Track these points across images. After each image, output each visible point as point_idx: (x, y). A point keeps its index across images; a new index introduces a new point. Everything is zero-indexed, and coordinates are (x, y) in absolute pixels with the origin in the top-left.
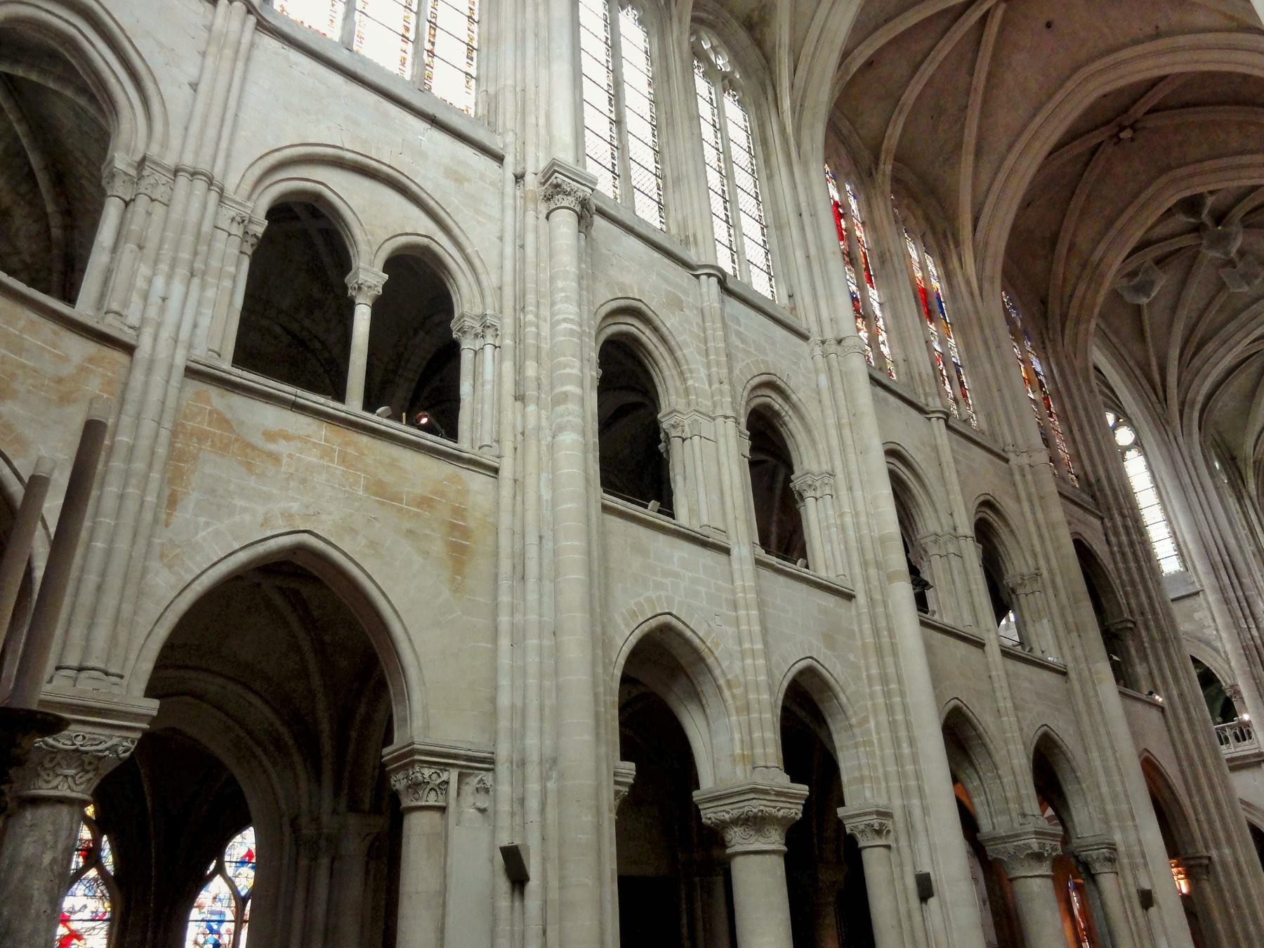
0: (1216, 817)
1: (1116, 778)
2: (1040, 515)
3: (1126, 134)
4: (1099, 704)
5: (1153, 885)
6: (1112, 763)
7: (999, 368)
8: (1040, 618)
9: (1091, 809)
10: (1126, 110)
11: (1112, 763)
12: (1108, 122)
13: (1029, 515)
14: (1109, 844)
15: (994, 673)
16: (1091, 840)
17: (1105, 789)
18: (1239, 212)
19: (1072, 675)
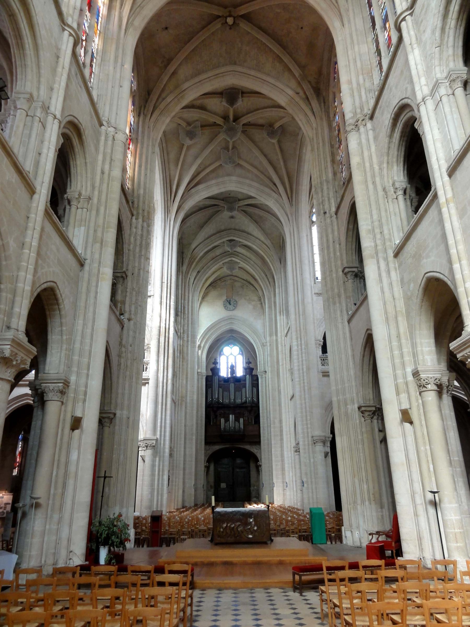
0: (127, 392)
1: (88, 341)
2: (107, 167)
3: (230, 21)
4: (96, 293)
5: (83, 414)
6: (89, 331)
7: (118, 76)
8: (80, 226)
9: (63, 355)
10: (236, 6)
11: (89, 331)
12: (225, 7)
13: (100, 162)
14: (65, 380)
15: (32, 216)
16: (52, 376)
17: (77, 345)
18: (244, 120)
19: (87, 267)
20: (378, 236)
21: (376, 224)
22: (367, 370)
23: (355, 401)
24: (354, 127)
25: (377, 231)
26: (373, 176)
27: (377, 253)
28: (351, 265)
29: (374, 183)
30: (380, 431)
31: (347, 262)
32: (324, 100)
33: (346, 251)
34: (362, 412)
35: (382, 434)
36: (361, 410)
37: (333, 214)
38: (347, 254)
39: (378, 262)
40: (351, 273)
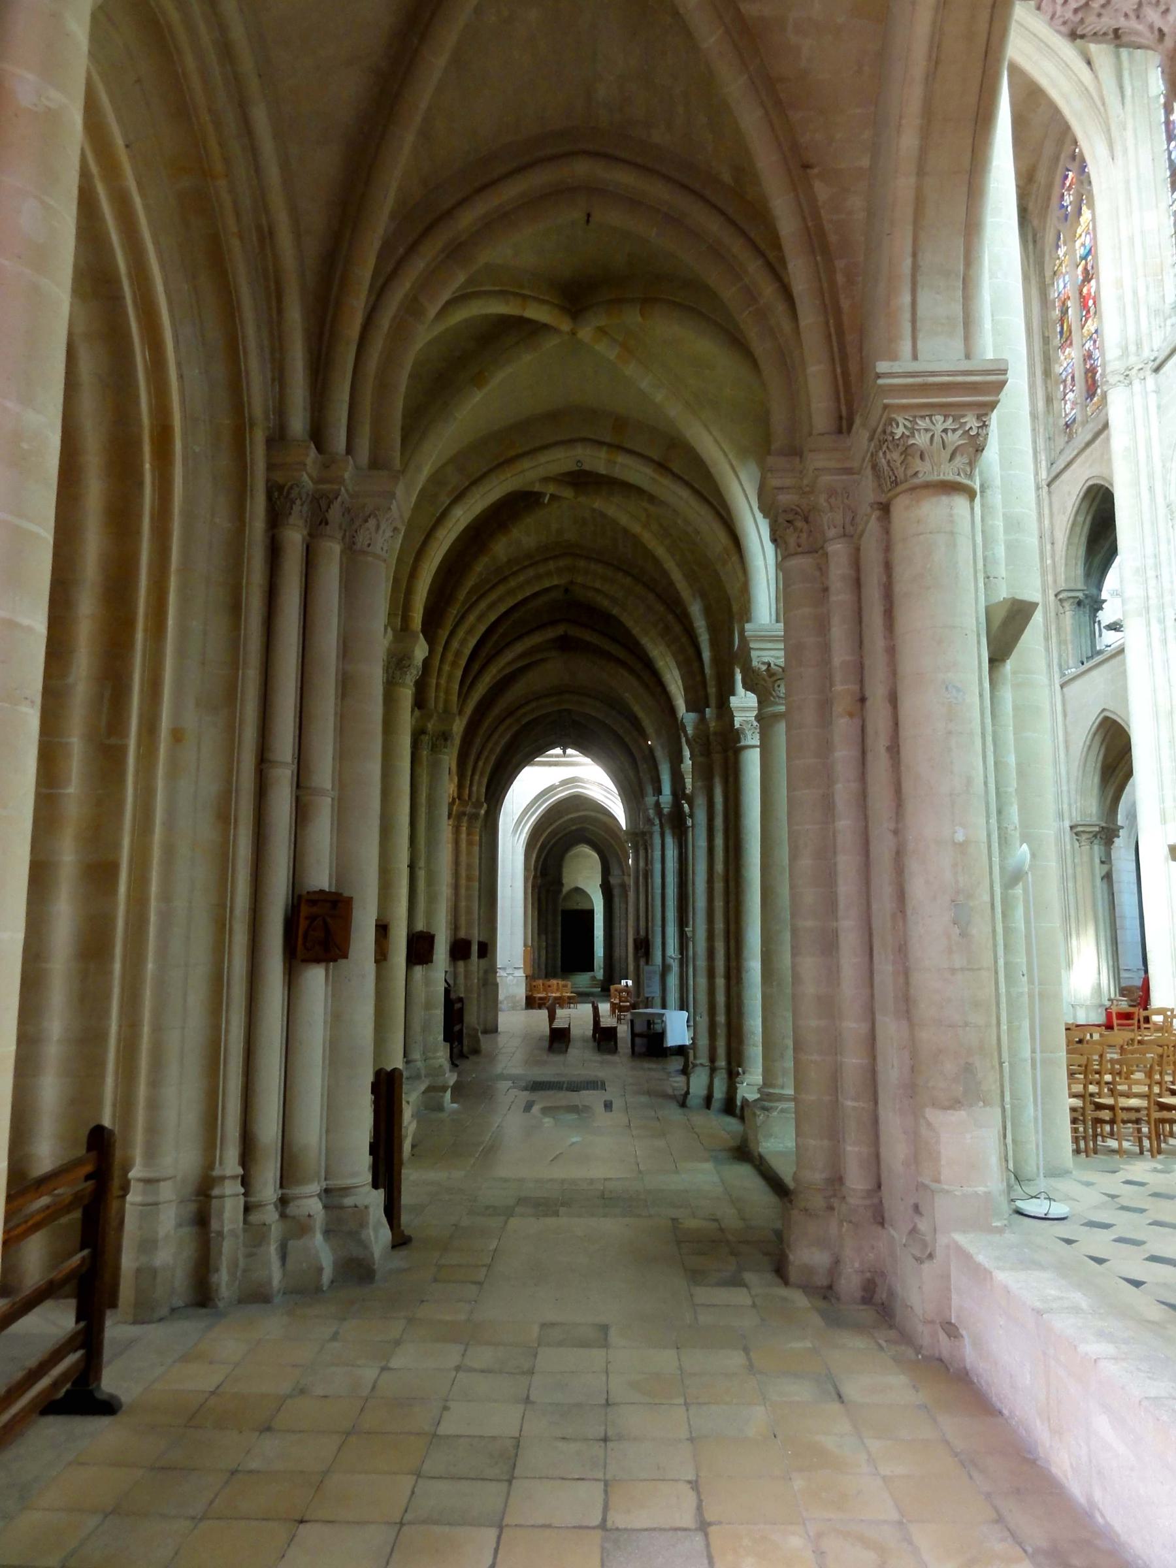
20: (1152, 583)
21: (1150, 562)
22: (1092, 769)
23: (1066, 815)
24: (1122, 378)
25: (1151, 573)
26: (1151, 476)
27: (1148, 610)
28: (1072, 586)
29: (1151, 489)
30: (1102, 862)
31: (1066, 580)
32: (1035, 236)
33: (1066, 559)
34: (1077, 834)
35: (1105, 868)
36: (1075, 830)
37: (1044, 484)
38: (1066, 565)
39: (1148, 624)
40: (1072, 600)
